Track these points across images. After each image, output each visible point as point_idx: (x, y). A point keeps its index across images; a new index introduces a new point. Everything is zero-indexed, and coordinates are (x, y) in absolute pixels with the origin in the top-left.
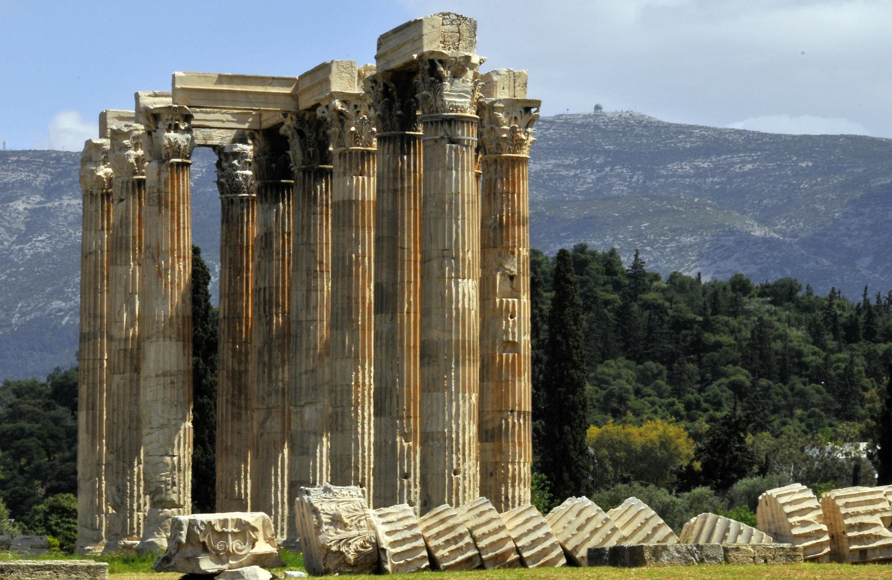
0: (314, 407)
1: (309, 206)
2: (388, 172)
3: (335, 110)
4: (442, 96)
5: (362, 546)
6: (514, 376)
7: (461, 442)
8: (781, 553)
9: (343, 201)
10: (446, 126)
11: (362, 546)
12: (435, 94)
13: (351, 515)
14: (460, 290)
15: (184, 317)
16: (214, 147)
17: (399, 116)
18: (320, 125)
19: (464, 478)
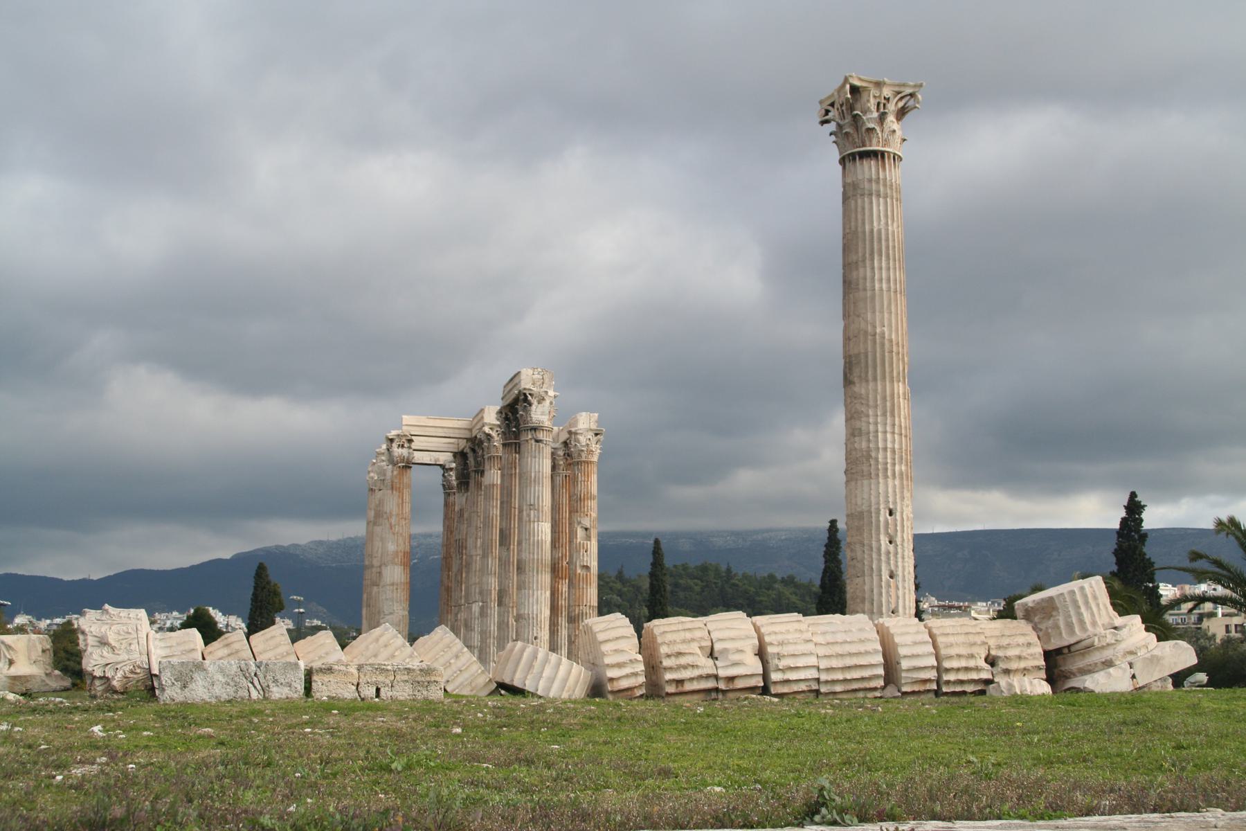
0: (477, 604)
1: (478, 491)
2: (508, 463)
3: (485, 433)
4: (530, 414)
5: (132, 672)
6: (587, 585)
7: (539, 620)
8: (406, 678)
9: (490, 485)
10: (533, 432)
11: (132, 672)
12: (527, 413)
13: (121, 637)
14: (540, 529)
15: (404, 553)
16: (440, 465)
17: (514, 432)
18: (481, 442)
19: (541, 641)
